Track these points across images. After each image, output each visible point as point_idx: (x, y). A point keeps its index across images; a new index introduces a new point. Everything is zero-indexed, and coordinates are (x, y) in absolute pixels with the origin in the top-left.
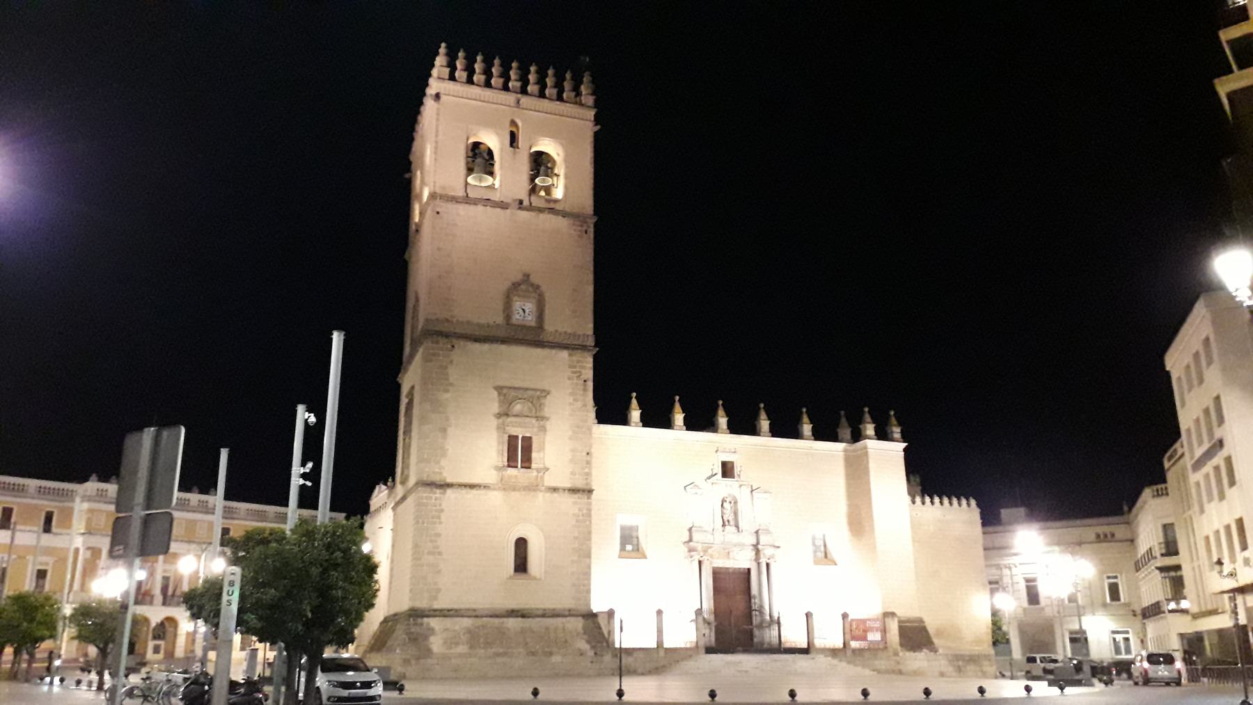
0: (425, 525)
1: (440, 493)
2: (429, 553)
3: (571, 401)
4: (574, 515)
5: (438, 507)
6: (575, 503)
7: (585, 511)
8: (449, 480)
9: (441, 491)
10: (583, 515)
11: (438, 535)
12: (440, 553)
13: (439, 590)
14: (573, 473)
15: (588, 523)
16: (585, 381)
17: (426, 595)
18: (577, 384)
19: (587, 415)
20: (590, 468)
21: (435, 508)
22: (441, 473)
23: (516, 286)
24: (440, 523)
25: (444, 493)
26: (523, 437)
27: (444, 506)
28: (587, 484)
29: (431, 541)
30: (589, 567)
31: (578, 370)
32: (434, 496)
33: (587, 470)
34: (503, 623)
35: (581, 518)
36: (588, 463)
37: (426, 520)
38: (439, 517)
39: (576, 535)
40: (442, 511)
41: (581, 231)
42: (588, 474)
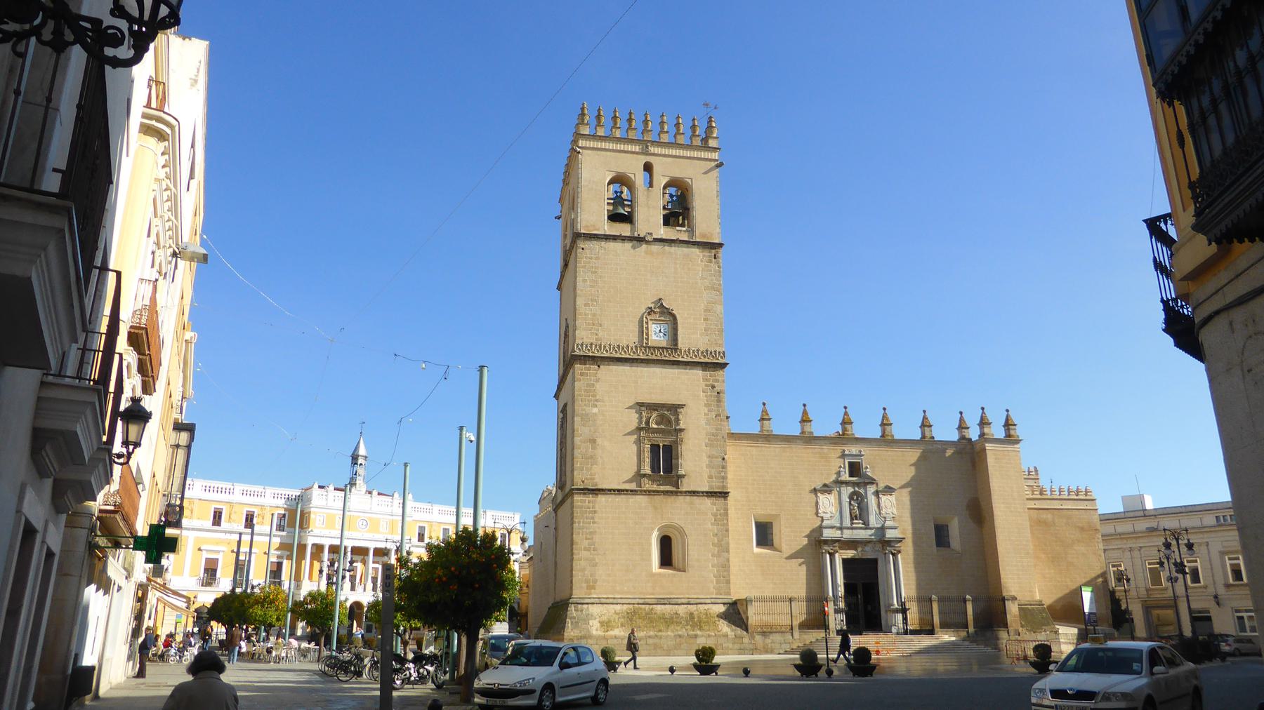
0: (581, 524)
2: (585, 549)
3: (706, 412)
7: (722, 511)
8: (600, 487)
10: (720, 515)
13: (595, 581)
14: (710, 477)
15: (725, 522)
16: (718, 393)
17: (584, 585)
18: (711, 396)
19: (720, 425)
20: (726, 473)
23: (650, 311)
24: (594, 523)
26: (664, 445)
28: (724, 487)
29: (586, 539)
30: (728, 560)
31: (711, 382)
33: (723, 474)
34: (652, 609)
36: (724, 467)
37: (582, 521)
38: (593, 518)
40: (595, 512)
41: (710, 256)
42: (725, 478)
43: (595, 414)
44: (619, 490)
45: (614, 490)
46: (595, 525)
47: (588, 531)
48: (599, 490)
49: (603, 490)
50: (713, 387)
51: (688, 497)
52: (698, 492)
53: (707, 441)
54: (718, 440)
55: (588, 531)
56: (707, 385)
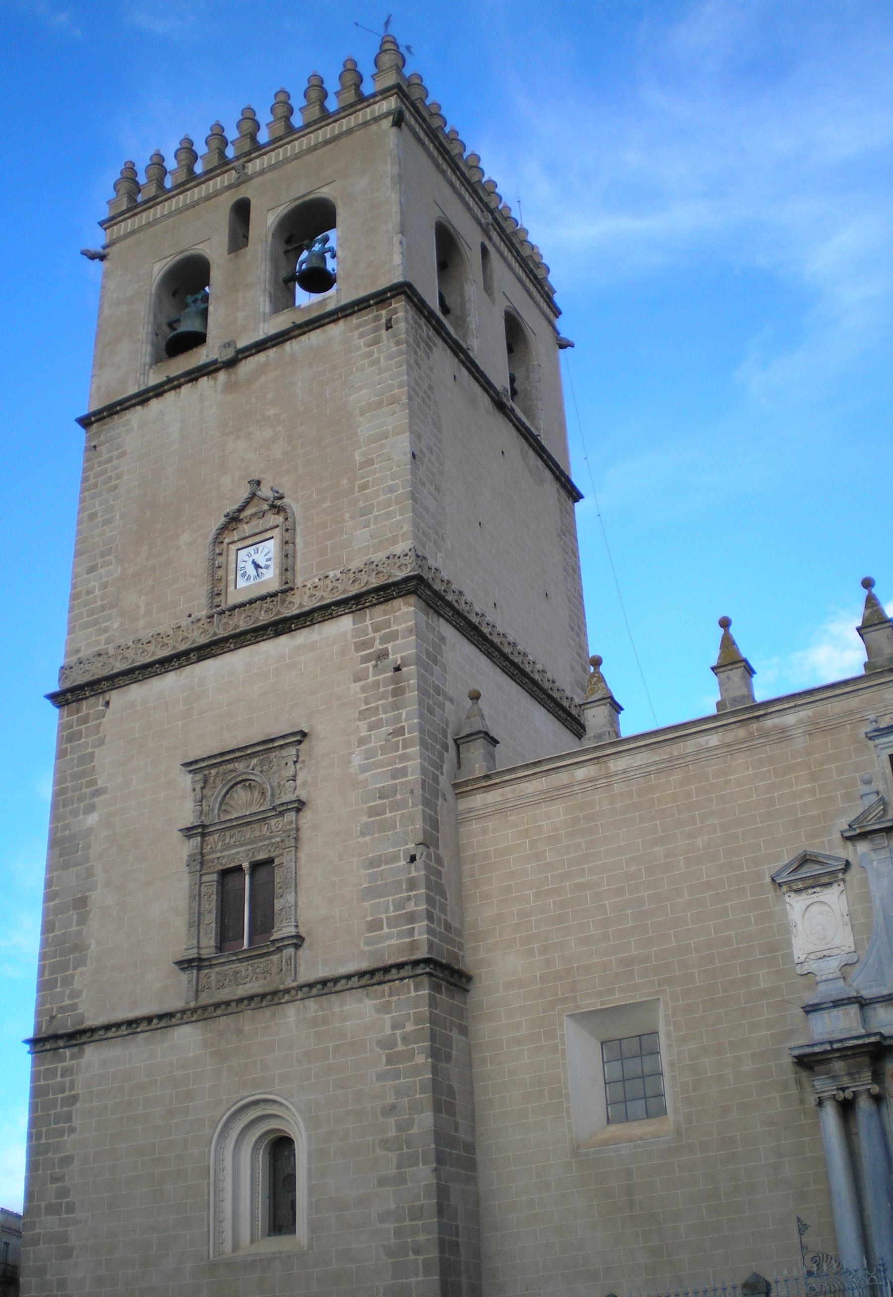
1: (73, 1057)
4: (379, 1043)
5: (67, 1094)
6: (385, 1008)
9: (76, 1049)
10: (405, 1040)
11: (67, 1161)
12: (70, 1208)
16: (397, 669)
18: (376, 684)
21: (60, 1096)
22: (74, 1007)
24: (72, 1130)
25: (81, 1053)
27: (79, 1090)
29: (55, 1179)
31: (378, 646)
32: (60, 1065)
35: (400, 1047)
38: (69, 1118)
39: (391, 1100)
40: (74, 1099)
43: (90, 829)
44: (130, 1023)
45: (118, 1025)
46: (75, 1136)
47: (57, 1156)
48: (83, 1032)
49: (93, 1030)
50: (382, 655)
51: (311, 1004)
52: (336, 980)
53: (365, 819)
54: (395, 807)
55: (57, 1156)
56: (366, 659)
